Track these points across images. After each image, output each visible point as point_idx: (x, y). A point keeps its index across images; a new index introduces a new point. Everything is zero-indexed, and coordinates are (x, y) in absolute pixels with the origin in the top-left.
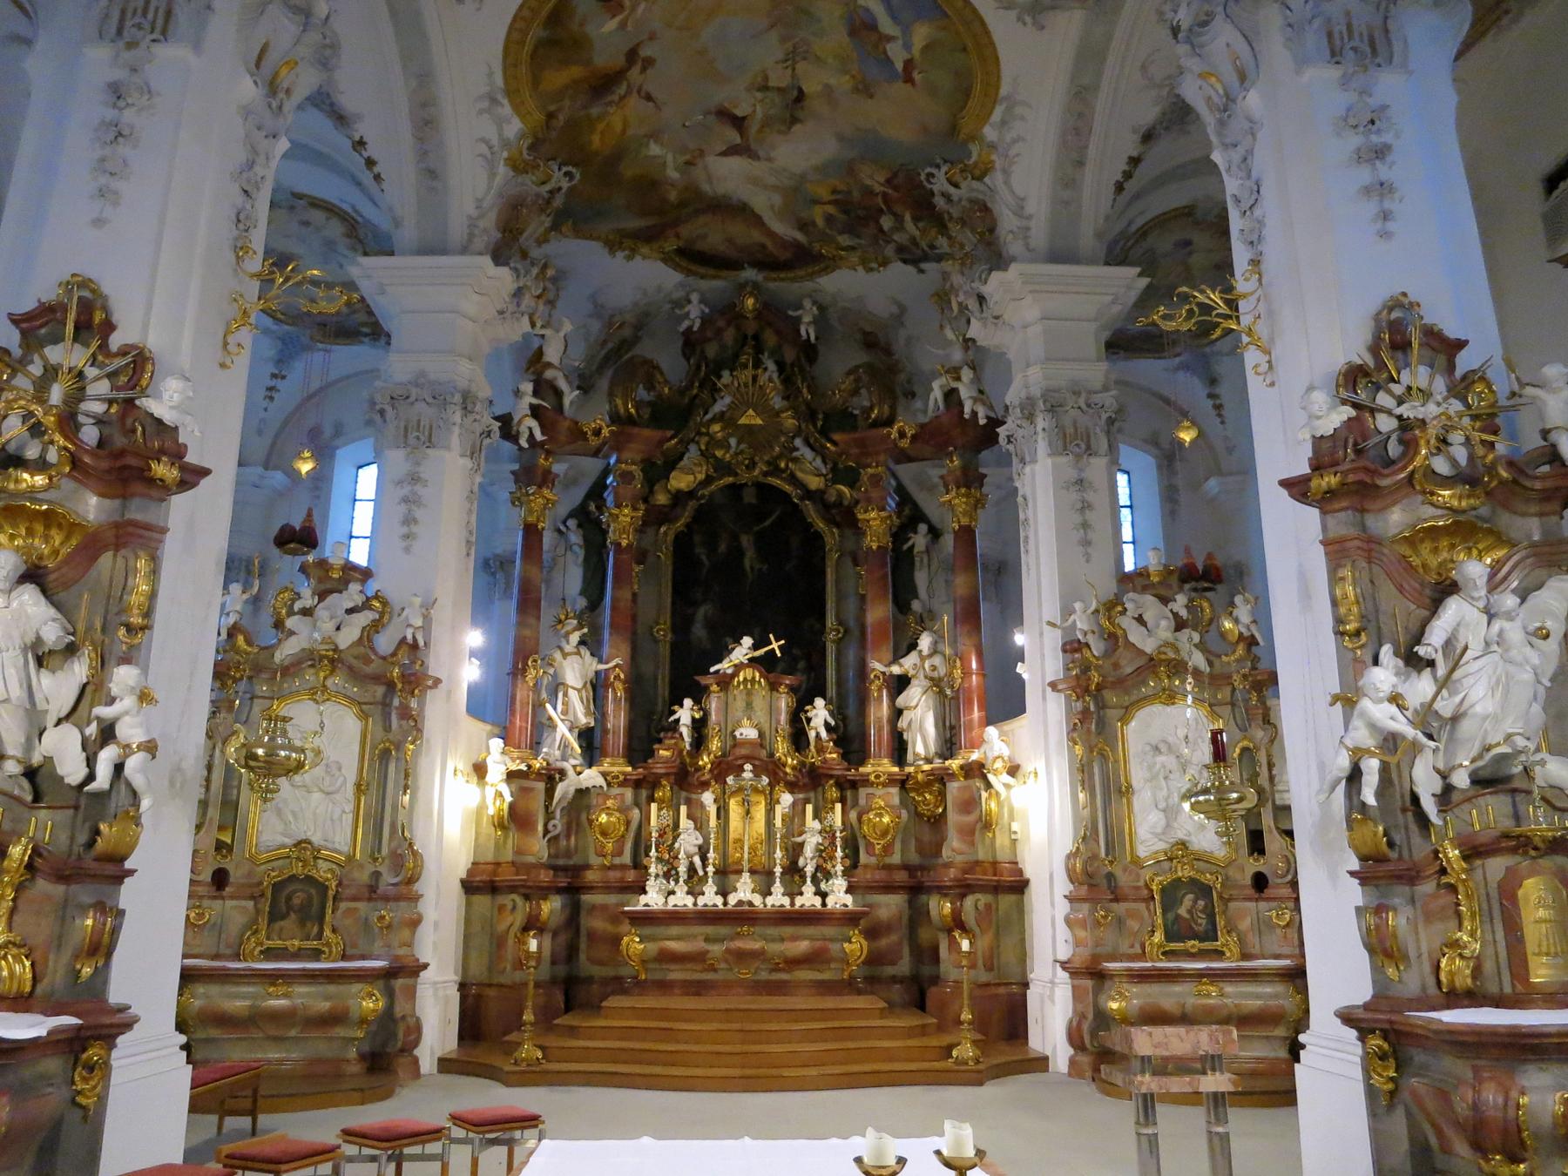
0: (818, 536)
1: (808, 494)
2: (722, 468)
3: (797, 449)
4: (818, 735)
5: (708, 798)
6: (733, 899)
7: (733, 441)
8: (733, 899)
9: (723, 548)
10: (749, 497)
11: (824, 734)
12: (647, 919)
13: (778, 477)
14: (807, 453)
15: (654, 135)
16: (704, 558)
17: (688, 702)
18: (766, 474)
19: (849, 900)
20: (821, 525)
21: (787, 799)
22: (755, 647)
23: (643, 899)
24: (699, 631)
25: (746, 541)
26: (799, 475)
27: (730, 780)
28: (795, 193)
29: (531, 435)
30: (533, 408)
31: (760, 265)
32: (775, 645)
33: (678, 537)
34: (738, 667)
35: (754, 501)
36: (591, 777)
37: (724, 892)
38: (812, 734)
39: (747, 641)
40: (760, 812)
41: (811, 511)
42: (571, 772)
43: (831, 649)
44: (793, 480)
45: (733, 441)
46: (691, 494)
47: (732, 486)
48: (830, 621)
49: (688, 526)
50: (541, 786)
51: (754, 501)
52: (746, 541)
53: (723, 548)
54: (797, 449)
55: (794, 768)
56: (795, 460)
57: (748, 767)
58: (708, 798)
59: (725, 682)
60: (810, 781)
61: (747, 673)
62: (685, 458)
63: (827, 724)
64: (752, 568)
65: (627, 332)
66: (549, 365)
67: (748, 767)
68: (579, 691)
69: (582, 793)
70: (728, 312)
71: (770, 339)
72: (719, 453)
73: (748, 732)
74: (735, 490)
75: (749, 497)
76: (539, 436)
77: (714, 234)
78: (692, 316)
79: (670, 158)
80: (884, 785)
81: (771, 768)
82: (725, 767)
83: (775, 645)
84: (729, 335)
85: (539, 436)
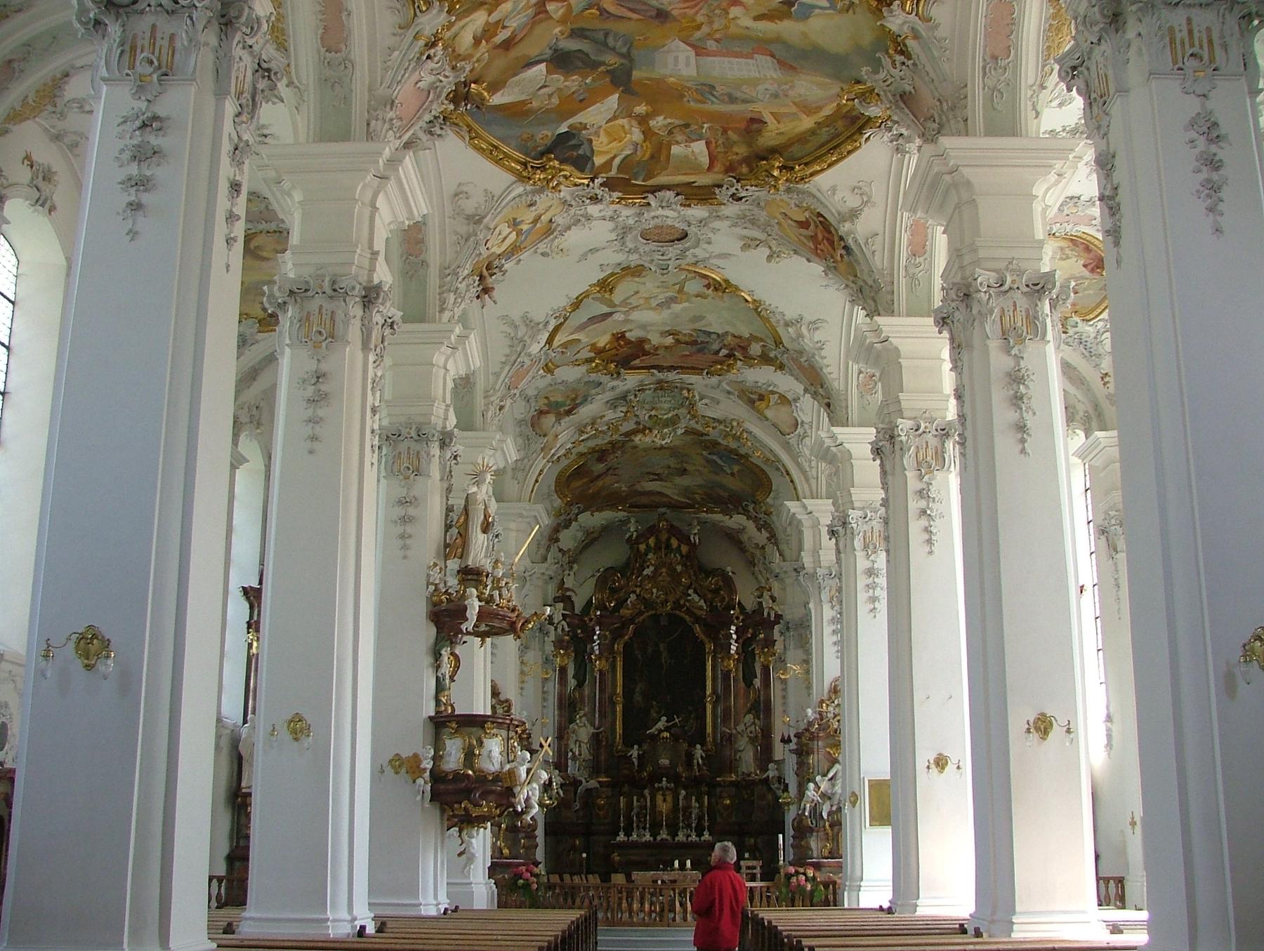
0: (703, 643)
1: (697, 620)
2: (648, 604)
3: (690, 595)
4: (698, 762)
5: (646, 792)
6: (659, 838)
7: (655, 591)
8: (659, 838)
9: (650, 650)
10: (664, 622)
11: (700, 762)
12: (621, 846)
13: (680, 611)
14: (696, 598)
15: (617, 482)
16: (639, 656)
17: (636, 747)
18: (672, 609)
19: (711, 838)
20: (702, 636)
21: (683, 793)
22: (667, 721)
23: (618, 839)
24: (638, 697)
25: (662, 647)
26: (692, 609)
27: (656, 785)
28: (686, 491)
29: (563, 629)
30: (563, 615)
31: (669, 507)
32: (677, 720)
33: (626, 645)
34: (661, 731)
35: (666, 624)
36: (593, 783)
37: (654, 835)
38: (695, 761)
39: (664, 718)
40: (669, 799)
41: (697, 628)
42: (584, 781)
43: (709, 707)
44: (689, 611)
45: (655, 591)
46: (631, 621)
47: (651, 615)
48: (709, 691)
49: (630, 639)
50: (572, 789)
51: (666, 624)
52: (662, 647)
53: (650, 650)
54: (690, 595)
55: (686, 778)
56: (688, 601)
57: (664, 779)
58: (646, 792)
59: (654, 738)
60: (694, 784)
61: (666, 734)
62: (629, 602)
63: (702, 757)
64: (666, 662)
65: (595, 535)
66: (568, 590)
67: (664, 779)
68: (586, 744)
69: (588, 791)
70: (653, 530)
71: (674, 542)
72: (647, 596)
73: (664, 762)
74: (656, 618)
75: (664, 622)
76: (567, 629)
77: (644, 500)
78: (632, 530)
79: (623, 486)
80: (728, 786)
81: (675, 778)
82: (655, 777)
83: (677, 720)
84: (652, 541)
85: (567, 629)
